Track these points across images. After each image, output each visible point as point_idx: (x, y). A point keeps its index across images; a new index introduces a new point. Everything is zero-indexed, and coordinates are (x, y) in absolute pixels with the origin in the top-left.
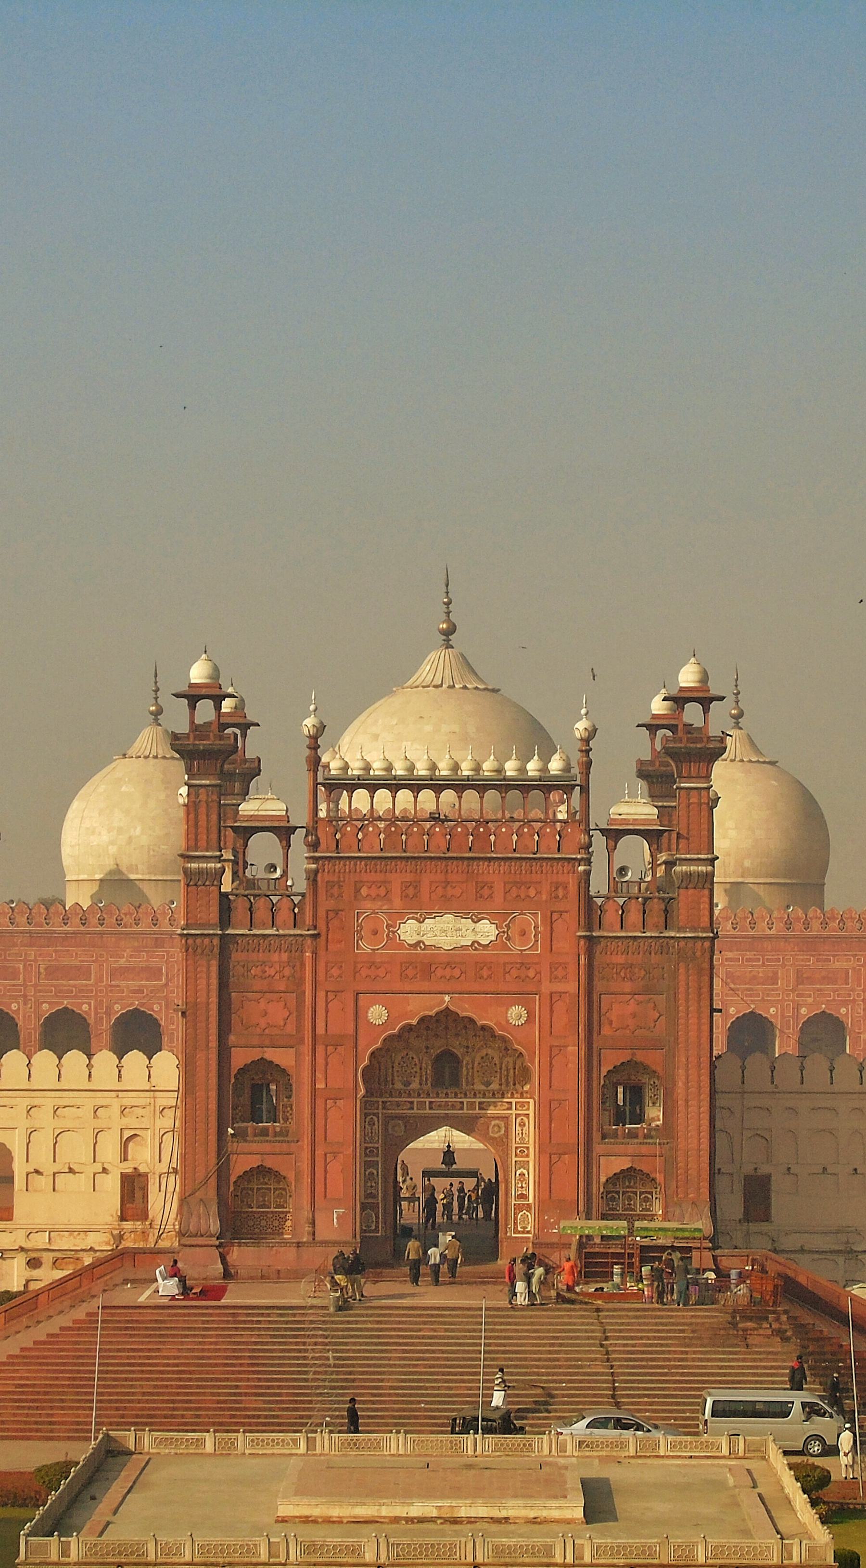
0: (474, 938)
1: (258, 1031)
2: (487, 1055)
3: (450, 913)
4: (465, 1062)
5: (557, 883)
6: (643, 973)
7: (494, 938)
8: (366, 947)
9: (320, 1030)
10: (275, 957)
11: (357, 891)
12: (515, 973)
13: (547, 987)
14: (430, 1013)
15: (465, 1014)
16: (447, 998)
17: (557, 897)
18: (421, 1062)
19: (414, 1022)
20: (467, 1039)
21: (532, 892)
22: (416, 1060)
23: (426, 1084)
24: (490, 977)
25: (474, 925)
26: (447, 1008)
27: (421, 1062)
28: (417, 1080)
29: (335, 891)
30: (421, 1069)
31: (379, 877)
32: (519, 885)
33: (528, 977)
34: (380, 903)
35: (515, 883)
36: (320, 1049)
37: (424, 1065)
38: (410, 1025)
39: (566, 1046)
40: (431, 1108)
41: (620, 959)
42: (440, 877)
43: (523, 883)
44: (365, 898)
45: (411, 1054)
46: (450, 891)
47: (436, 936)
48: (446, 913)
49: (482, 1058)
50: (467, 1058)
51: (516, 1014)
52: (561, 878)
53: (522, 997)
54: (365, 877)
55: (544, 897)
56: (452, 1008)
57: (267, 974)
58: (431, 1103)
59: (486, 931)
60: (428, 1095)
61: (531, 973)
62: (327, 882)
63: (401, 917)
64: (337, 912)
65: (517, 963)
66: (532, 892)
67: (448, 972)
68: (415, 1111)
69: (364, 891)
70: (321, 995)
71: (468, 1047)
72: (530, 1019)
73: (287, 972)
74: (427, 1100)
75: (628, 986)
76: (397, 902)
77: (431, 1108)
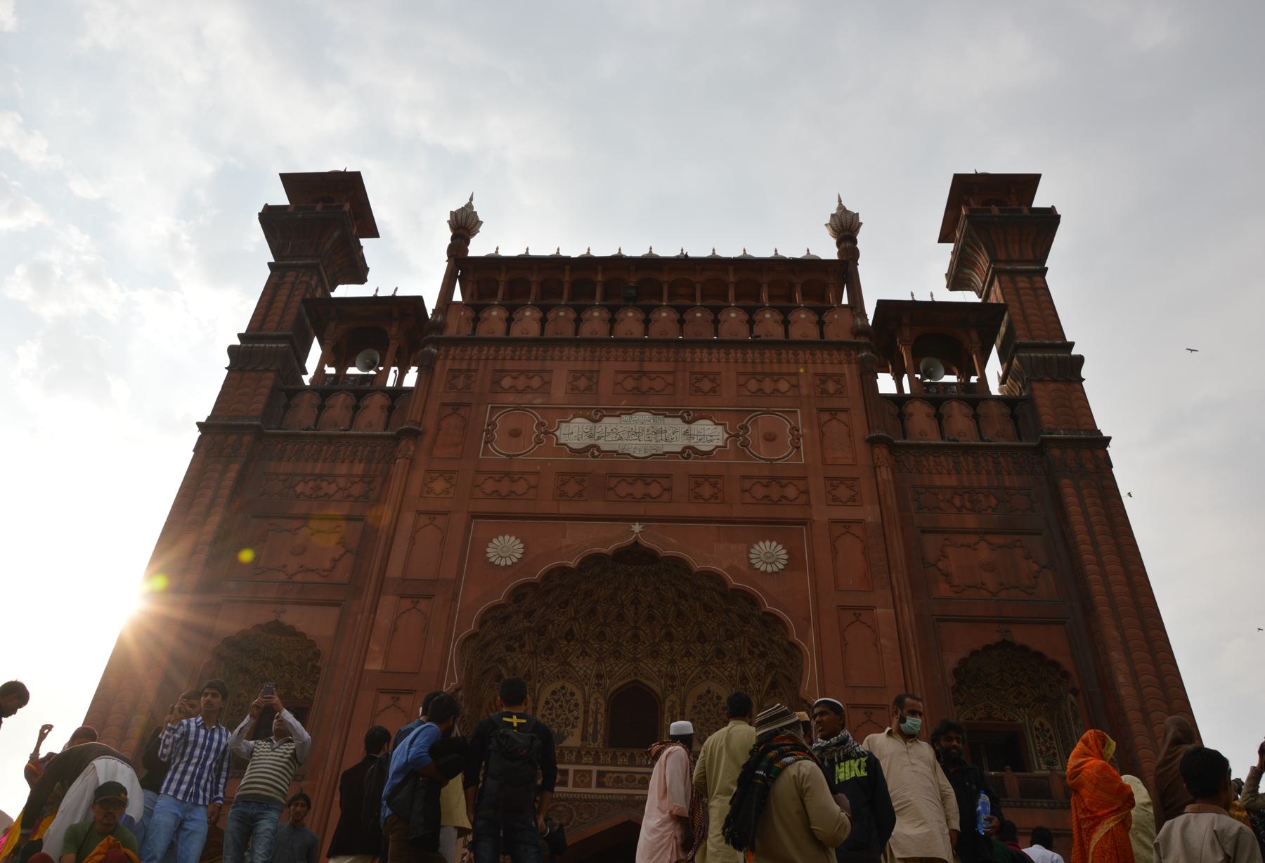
0: (686, 443)
1: (282, 577)
2: (709, 692)
3: (647, 411)
4: (668, 704)
5: (824, 375)
6: (993, 502)
7: (721, 444)
8: (498, 450)
9: (395, 570)
10: (343, 469)
11: (496, 382)
12: (759, 492)
13: (822, 513)
14: (604, 551)
15: (669, 552)
16: (637, 528)
17: (824, 392)
18: (587, 703)
19: (573, 564)
20: (672, 662)
21: (783, 386)
22: (578, 696)
23: (595, 740)
24: (714, 496)
25: (686, 426)
26: (636, 543)
27: (587, 703)
28: (577, 732)
29: (460, 382)
30: (586, 712)
31: (536, 365)
32: (759, 377)
33: (785, 497)
34: (530, 396)
35: (754, 374)
36: (388, 603)
37: (592, 706)
38: (563, 570)
39: (871, 608)
40: (600, 784)
41: (952, 481)
42: (634, 366)
43: (765, 374)
44: (506, 391)
45: (570, 687)
46: (645, 384)
47: (621, 439)
48: (638, 410)
49: (700, 697)
50: (672, 697)
51: (768, 554)
52: (829, 369)
53: (771, 527)
54: (509, 365)
55: (804, 391)
56: (645, 542)
57: (322, 493)
58: (601, 774)
59: (709, 435)
60: (596, 762)
61: (791, 492)
62: (451, 370)
63: (566, 413)
64: (456, 406)
65: (764, 477)
66: (783, 386)
67: (639, 489)
68: (570, 788)
69: (507, 382)
70: (408, 519)
71: (673, 678)
72: (794, 562)
73: (357, 490)
74: (595, 769)
75: (971, 521)
76: (559, 393)
77: (600, 784)
